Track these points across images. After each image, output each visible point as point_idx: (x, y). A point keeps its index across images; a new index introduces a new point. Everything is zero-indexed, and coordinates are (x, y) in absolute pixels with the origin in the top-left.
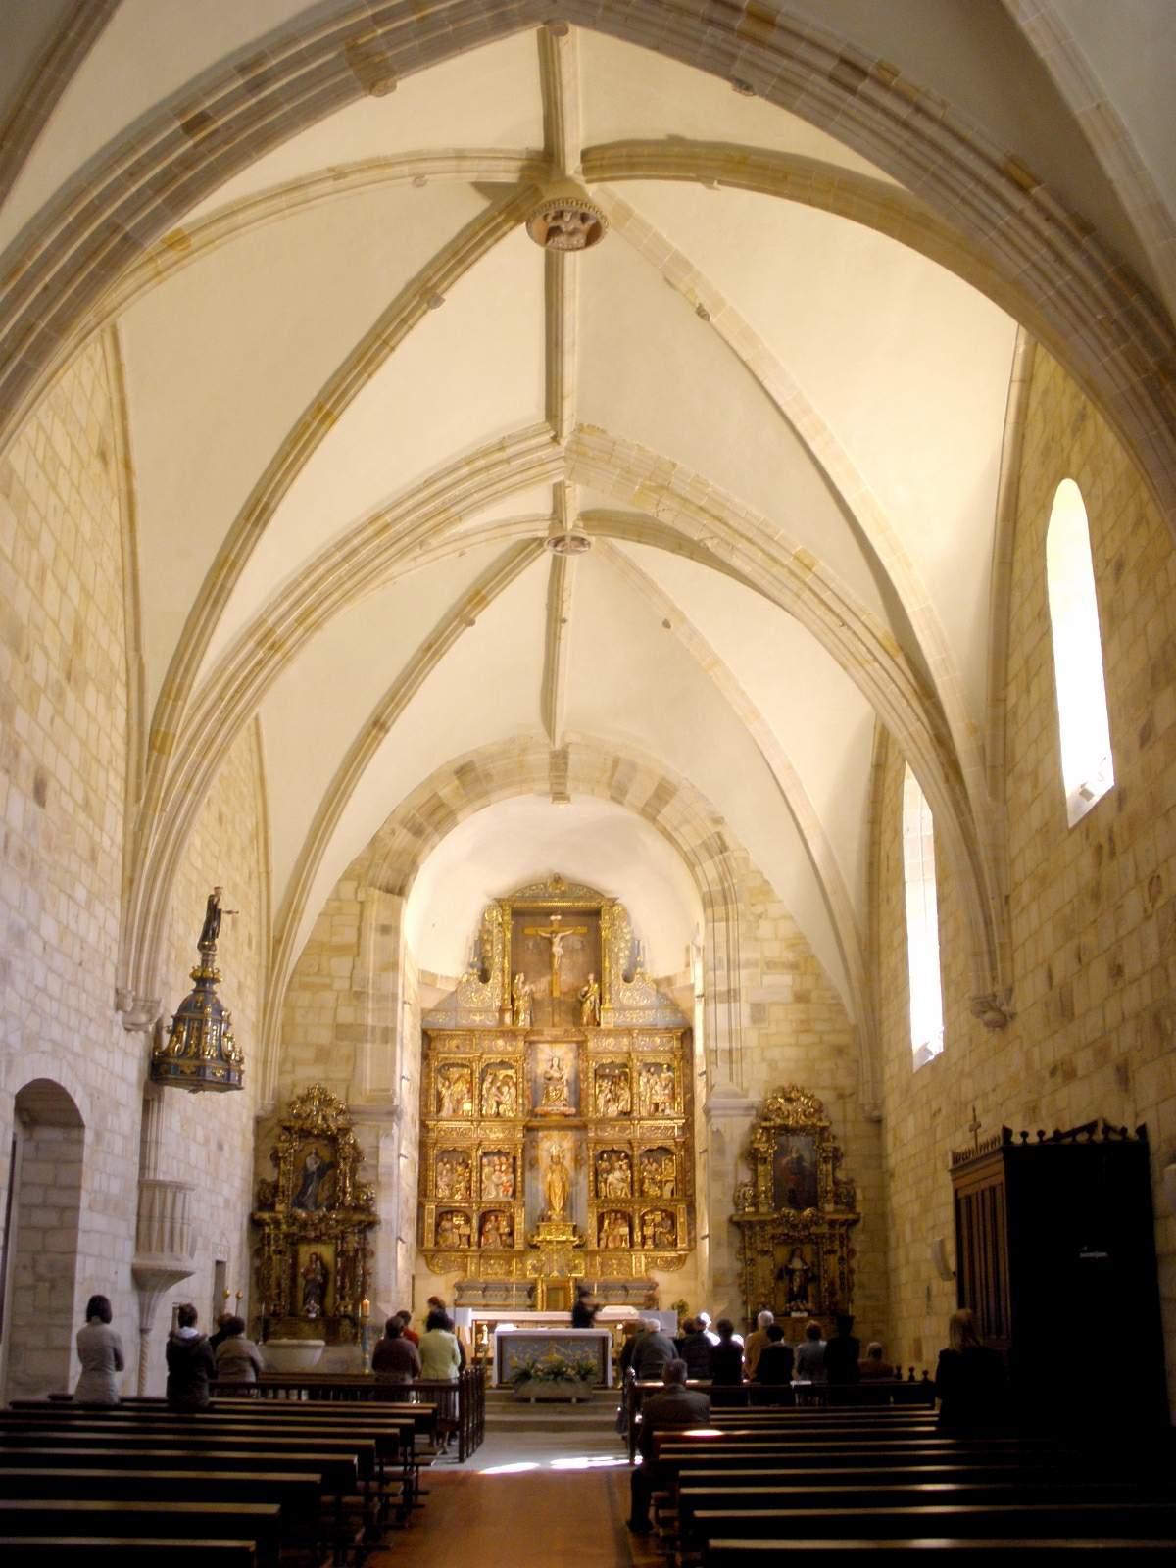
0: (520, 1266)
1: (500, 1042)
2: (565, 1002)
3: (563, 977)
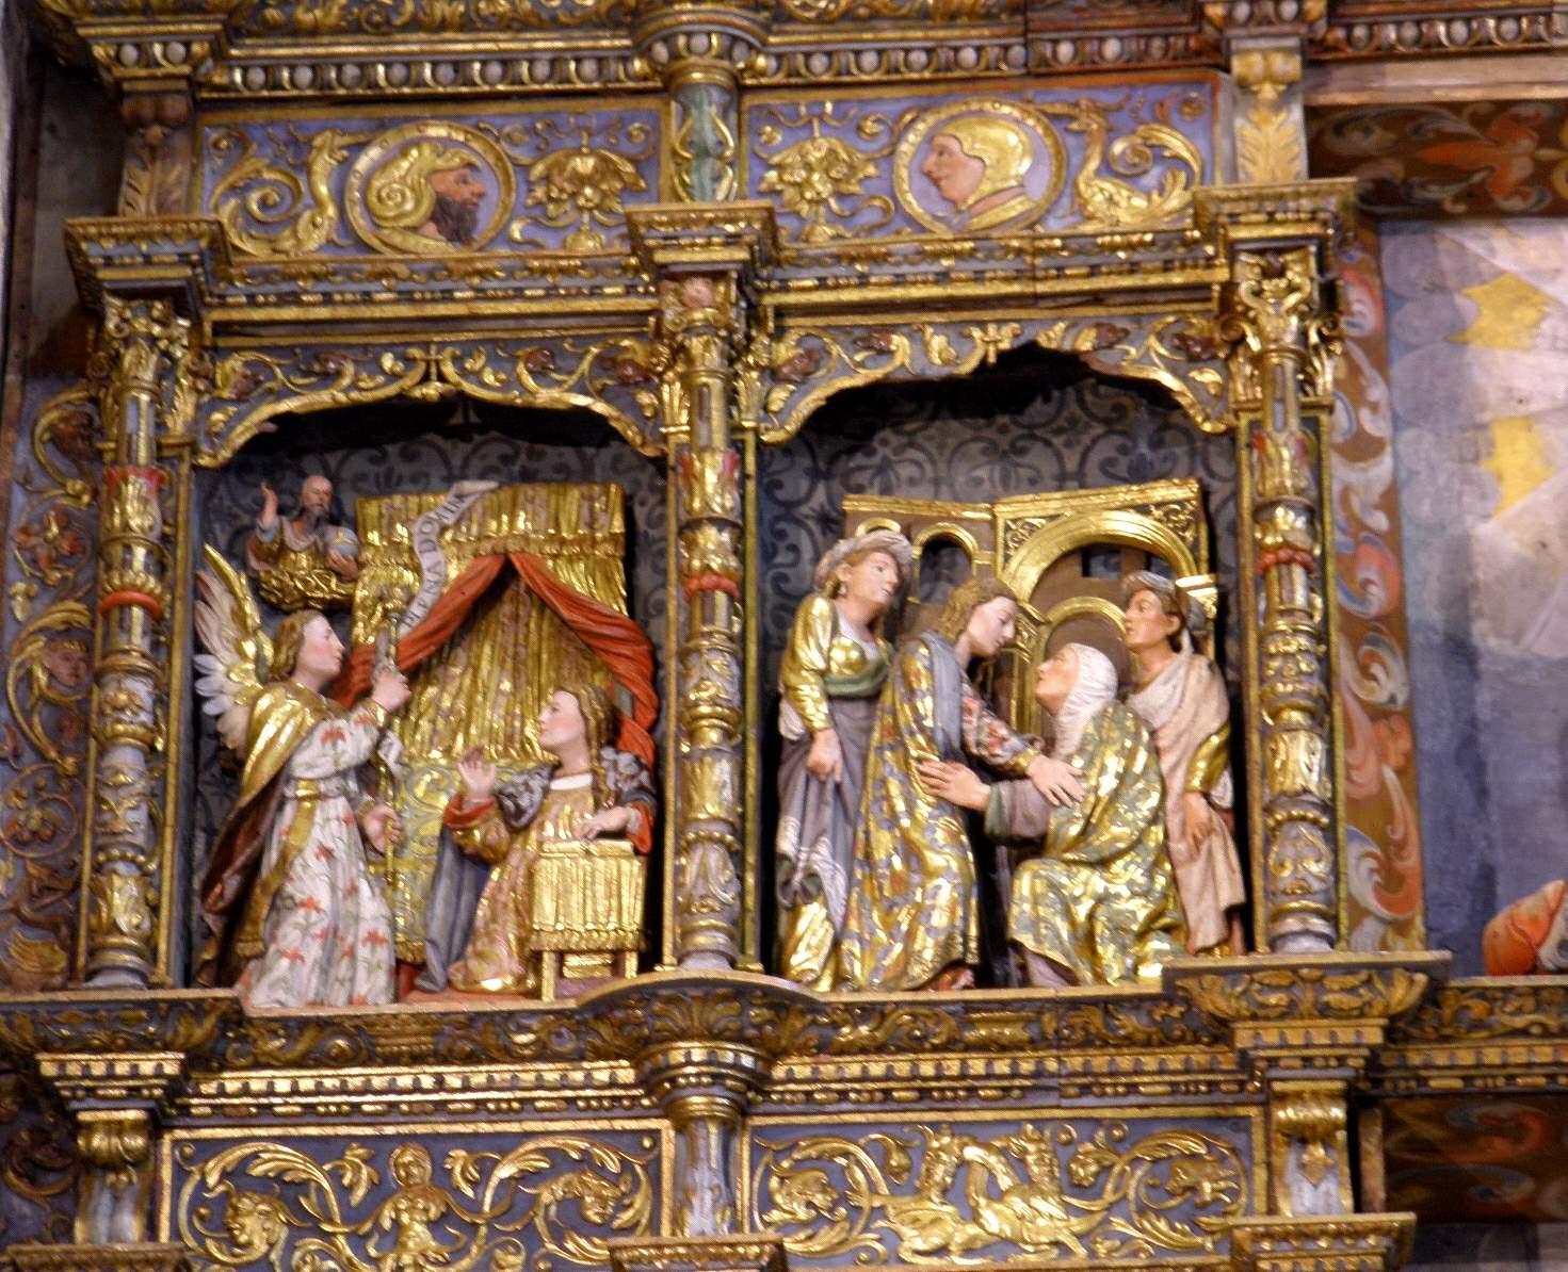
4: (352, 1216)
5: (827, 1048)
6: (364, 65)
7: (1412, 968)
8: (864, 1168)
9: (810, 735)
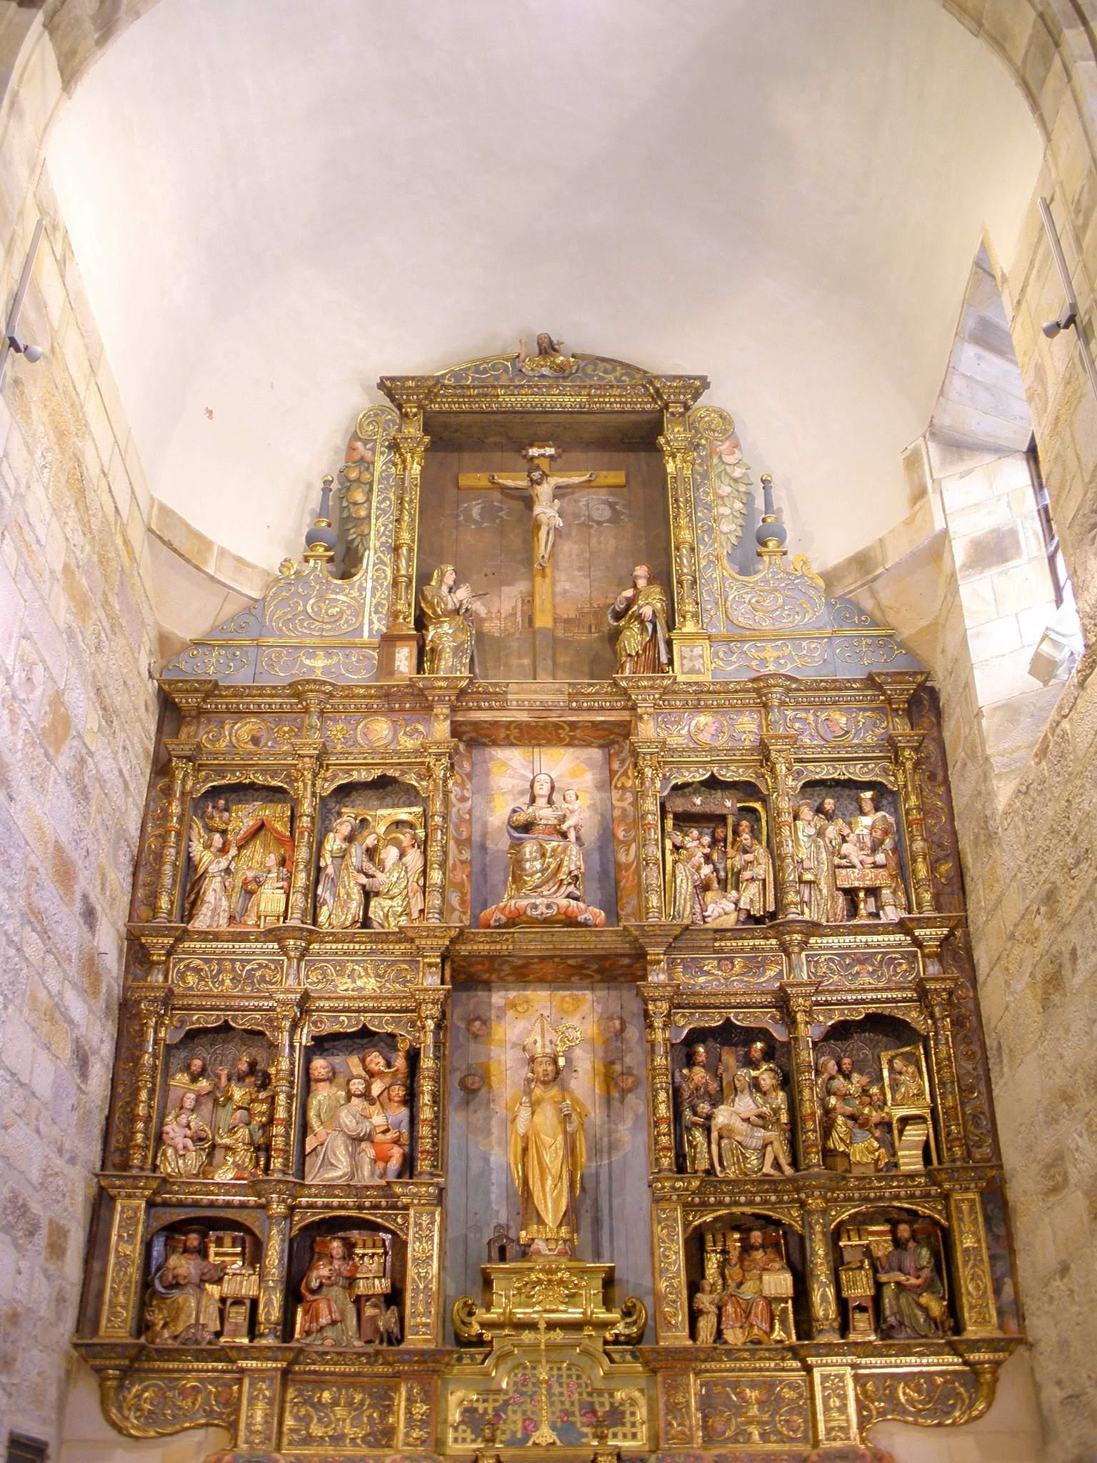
0: (420, 1409)
1: (381, 728)
2: (567, 644)
3: (564, 584)
4: (213, 977)
5: (322, 942)
6: (238, 704)
8: (331, 970)
9: (327, 866)
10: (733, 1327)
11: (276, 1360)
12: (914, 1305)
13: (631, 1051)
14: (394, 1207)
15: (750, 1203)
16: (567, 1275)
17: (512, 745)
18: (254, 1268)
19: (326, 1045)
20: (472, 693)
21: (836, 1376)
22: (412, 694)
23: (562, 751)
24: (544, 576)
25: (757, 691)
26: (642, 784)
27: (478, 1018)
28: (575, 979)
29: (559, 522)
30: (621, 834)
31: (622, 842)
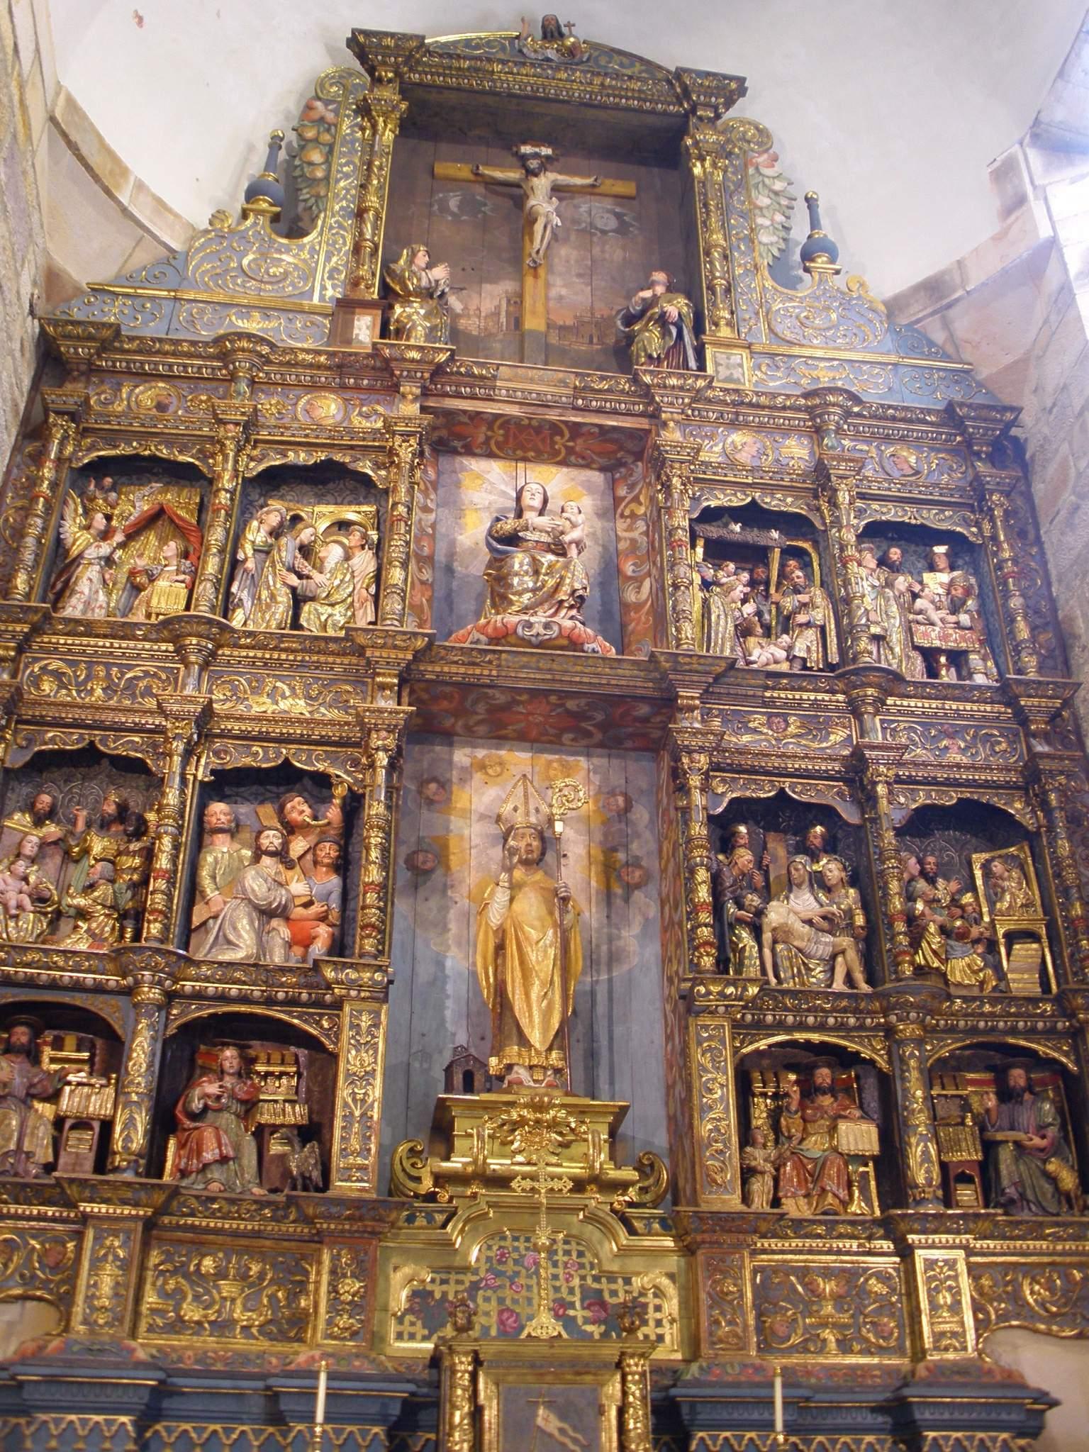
0: (351, 1286)
1: (329, 408)
3: (558, 289)
4: (78, 684)
5: (237, 646)
6: (142, 363)
7: (424, 635)
9: (246, 560)
10: (794, 1196)
11: (136, 1205)
12: (1038, 1174)
13: (638, 836)
14: (318, 1003)
15: (821, 1027)
16: (562, 1114)
17: (491, 455)
18: (109, 1079)
19: (227, 791)
20: (452, 373)
21: (946, 1262)
22: (373, 368)
23: (553, 469)
24: (536, 276)
25: (809, 410)
26: (669, 495)
27: (435, 780)
28: (567, 737)
29: (557, 221)
30: (629, 569)
31: (630, 578)
